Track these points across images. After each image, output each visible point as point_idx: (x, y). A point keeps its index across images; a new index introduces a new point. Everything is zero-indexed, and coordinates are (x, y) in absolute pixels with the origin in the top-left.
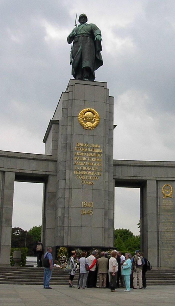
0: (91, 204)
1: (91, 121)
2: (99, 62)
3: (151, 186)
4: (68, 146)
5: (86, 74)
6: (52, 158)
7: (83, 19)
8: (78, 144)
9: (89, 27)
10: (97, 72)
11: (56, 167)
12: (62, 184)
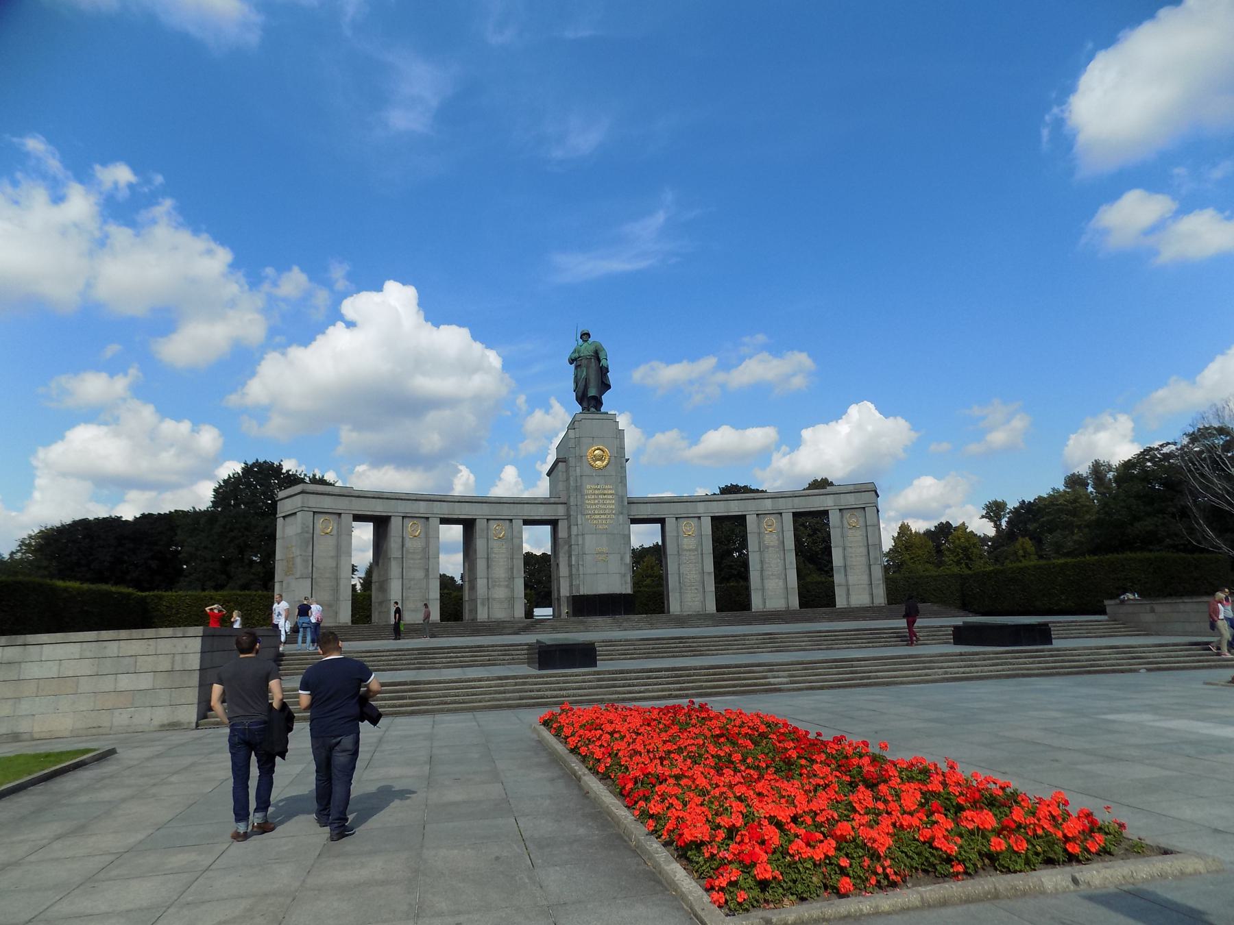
0: (605, 549)
1: (601, 459)
2: (606, 386)
3: (670, 523)
4: (579, 489)
5: (593, 403)
6: (561, 500)
7: (585, 336)
8: (588, 487)
9: (592, 348)
10: (605, 398)
11: (568, 510)
12: (574, 530)
